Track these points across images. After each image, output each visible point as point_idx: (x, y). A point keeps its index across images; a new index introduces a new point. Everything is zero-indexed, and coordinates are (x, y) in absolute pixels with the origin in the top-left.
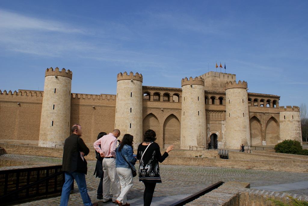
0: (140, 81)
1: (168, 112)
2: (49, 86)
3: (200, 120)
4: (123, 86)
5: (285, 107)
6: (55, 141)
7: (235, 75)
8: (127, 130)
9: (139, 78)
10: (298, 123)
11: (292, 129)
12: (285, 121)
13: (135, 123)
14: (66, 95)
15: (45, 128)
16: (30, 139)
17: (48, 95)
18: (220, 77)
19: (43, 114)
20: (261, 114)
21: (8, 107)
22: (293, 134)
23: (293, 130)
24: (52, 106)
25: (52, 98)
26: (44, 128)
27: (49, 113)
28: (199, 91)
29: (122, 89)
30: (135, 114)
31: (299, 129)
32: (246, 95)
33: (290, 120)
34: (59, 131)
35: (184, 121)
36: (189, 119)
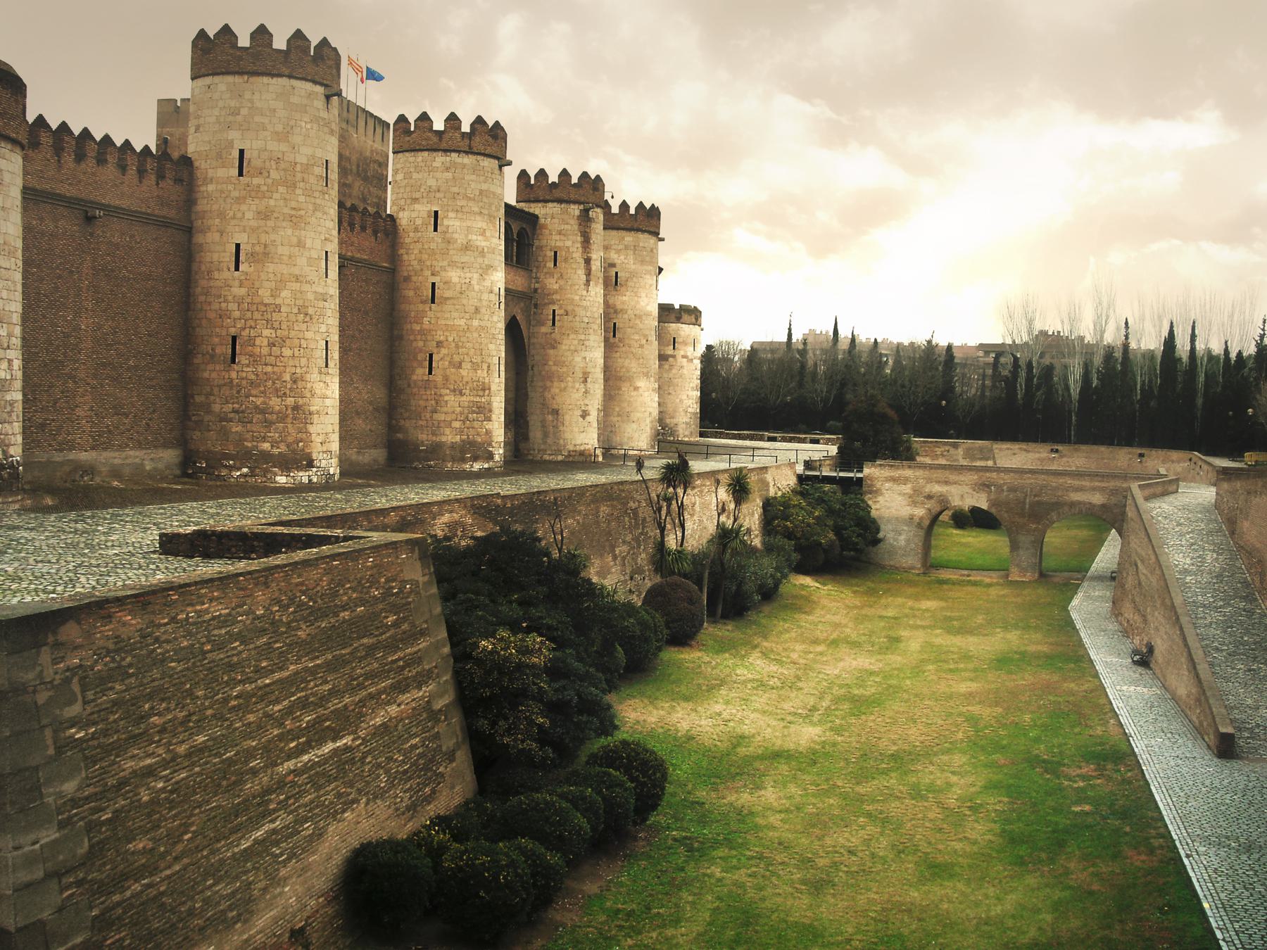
2: (297, 139)
4: (473, 185)
5: (677, 307)
8: (494, 388)
12: (674, 357)
15: (295, 382)
16: (139, 446)
17: (298, 191)
19: (266, 301)
21: (43, 234)
24: (319, 258)
25: (319, 214)
26: (287, 377)
27: (310, 296)
29: (470, 199)
35: (554, 348)
36: (576, 342)
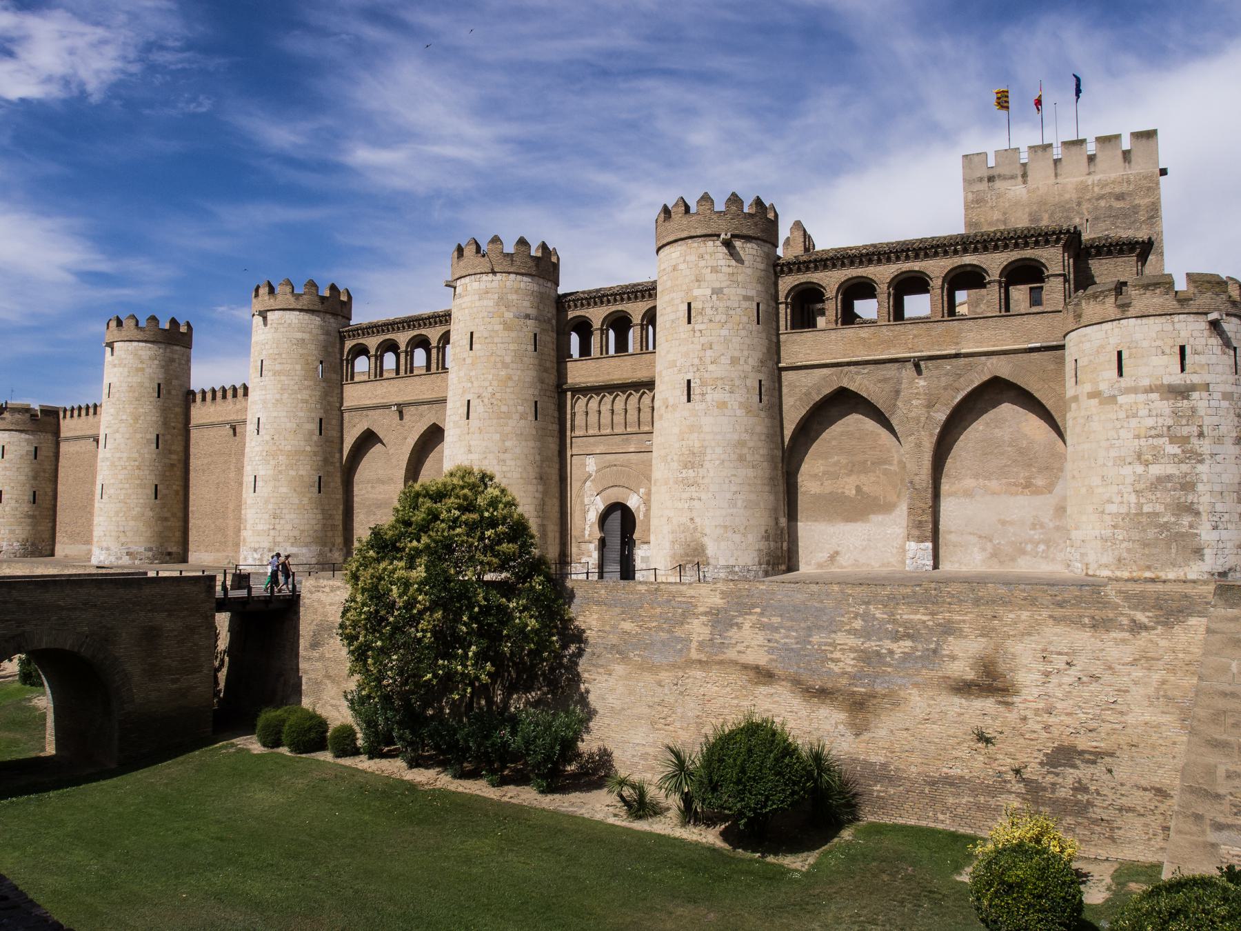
0: (301, 310)
1: (421, 415)
3: (472, 443)
6: (105, 545)
7: (1150, 135)
9: (292, 299)
10: (1164, 406)
11: (1113, 453)
13: (271, 472)
14: (137, 400)
18: (1024, 175)
20: (890, 371)
22: (1115, 488)
23: (1121, 461)
28: (477, 304)
30: (267, 438)
31: (1174, 449)
32: (715, 270)
33: (1103, 387)
34: (117, 513)
